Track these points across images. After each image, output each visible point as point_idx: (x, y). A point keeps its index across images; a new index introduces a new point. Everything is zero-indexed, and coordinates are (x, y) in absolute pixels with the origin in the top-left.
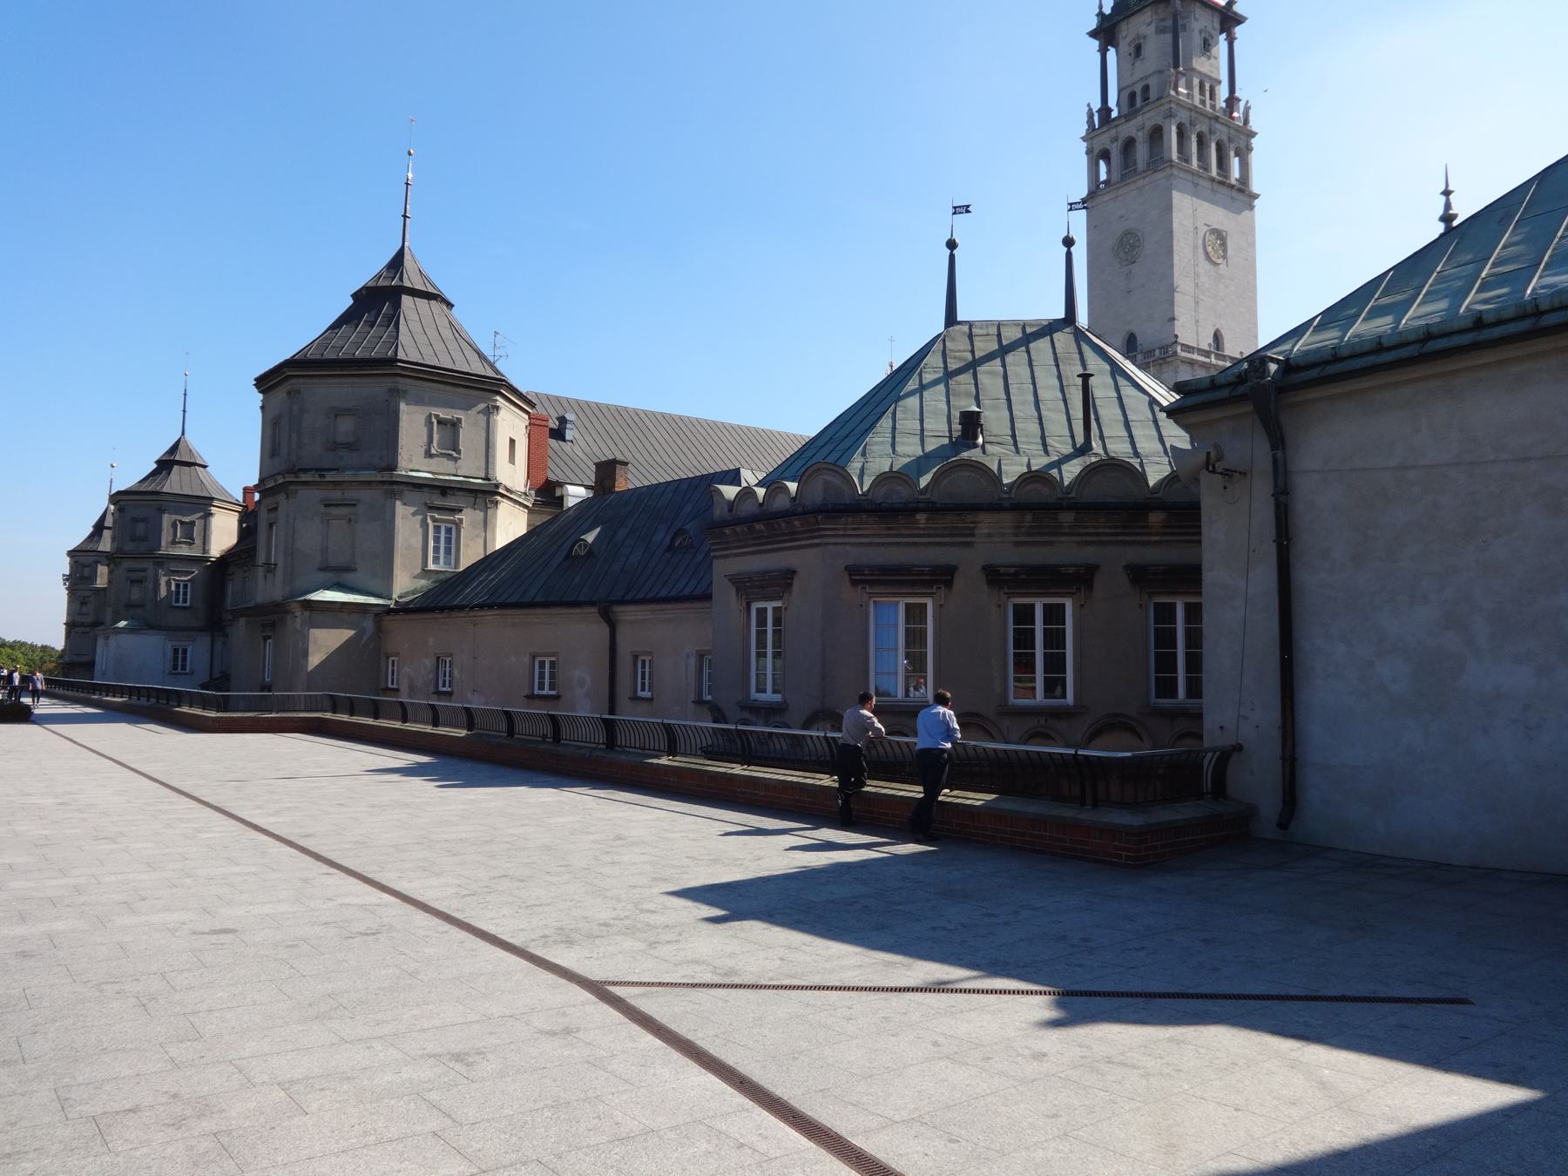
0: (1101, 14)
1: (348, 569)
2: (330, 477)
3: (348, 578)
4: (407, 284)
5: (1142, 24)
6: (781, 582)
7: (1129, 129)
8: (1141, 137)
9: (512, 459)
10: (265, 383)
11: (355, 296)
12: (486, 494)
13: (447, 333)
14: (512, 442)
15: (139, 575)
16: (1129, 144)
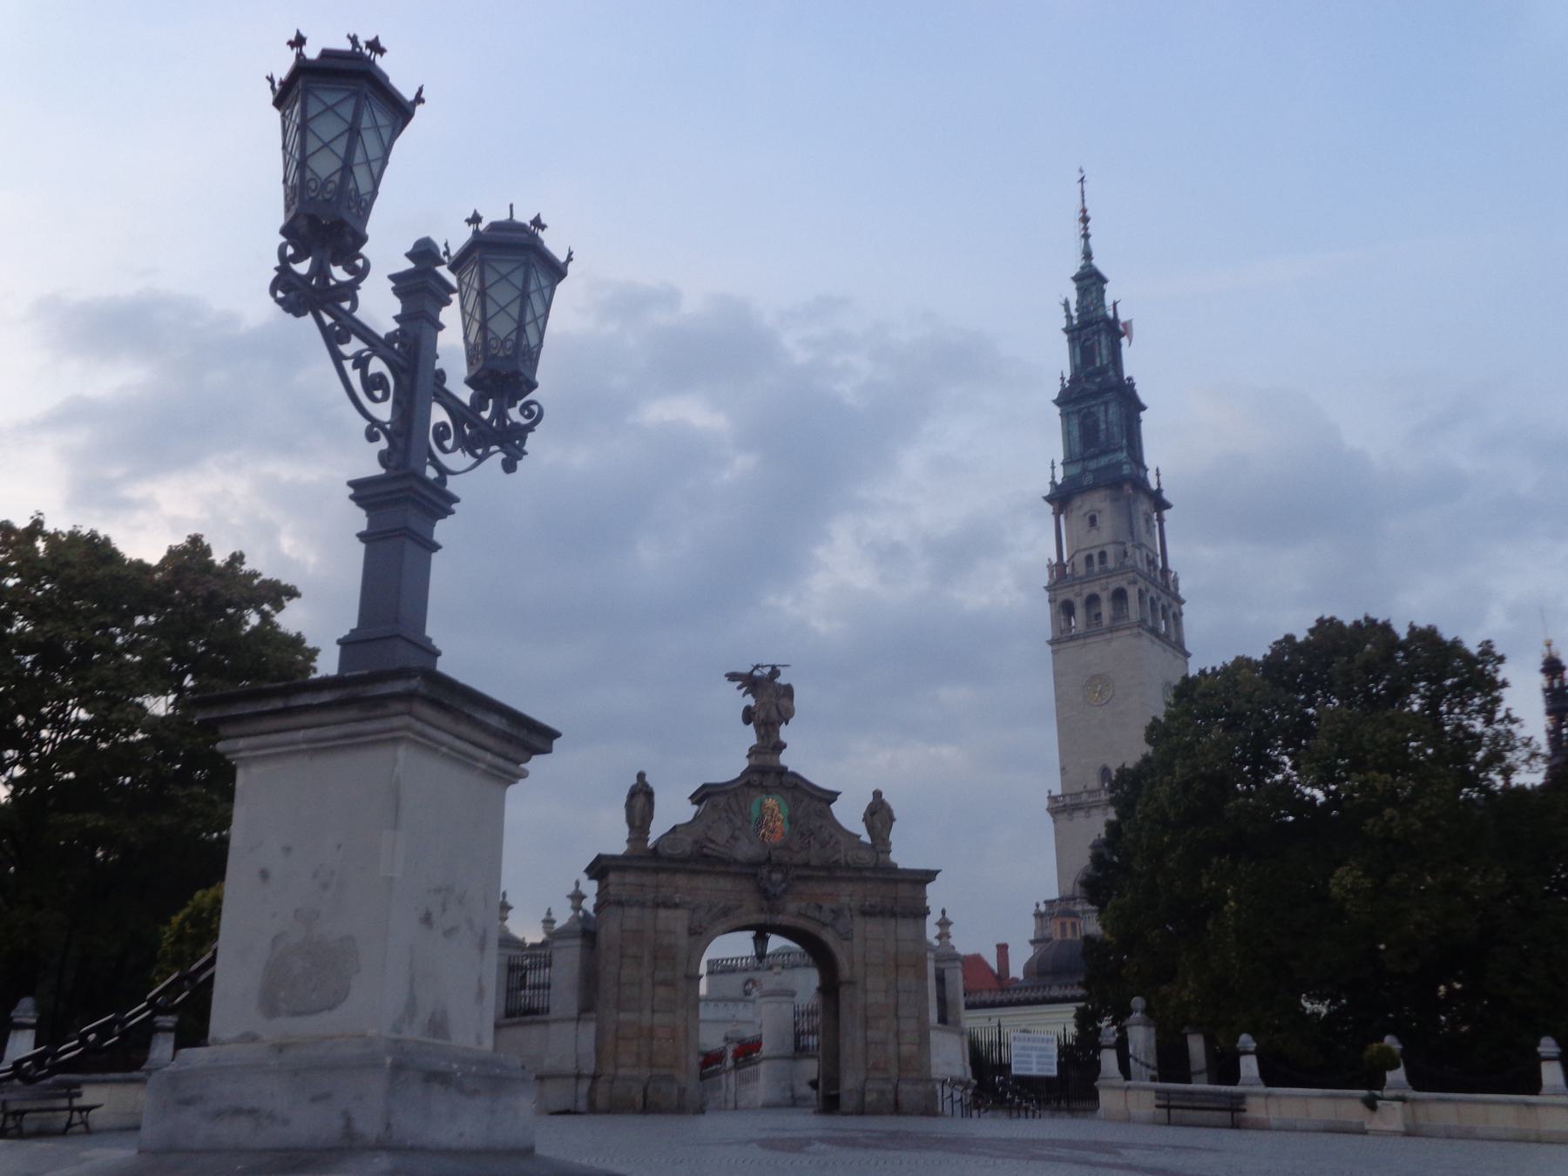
0: (1053, 483)
5: (1098, 502)
8: (1105, 597)
16: (1093, 600)
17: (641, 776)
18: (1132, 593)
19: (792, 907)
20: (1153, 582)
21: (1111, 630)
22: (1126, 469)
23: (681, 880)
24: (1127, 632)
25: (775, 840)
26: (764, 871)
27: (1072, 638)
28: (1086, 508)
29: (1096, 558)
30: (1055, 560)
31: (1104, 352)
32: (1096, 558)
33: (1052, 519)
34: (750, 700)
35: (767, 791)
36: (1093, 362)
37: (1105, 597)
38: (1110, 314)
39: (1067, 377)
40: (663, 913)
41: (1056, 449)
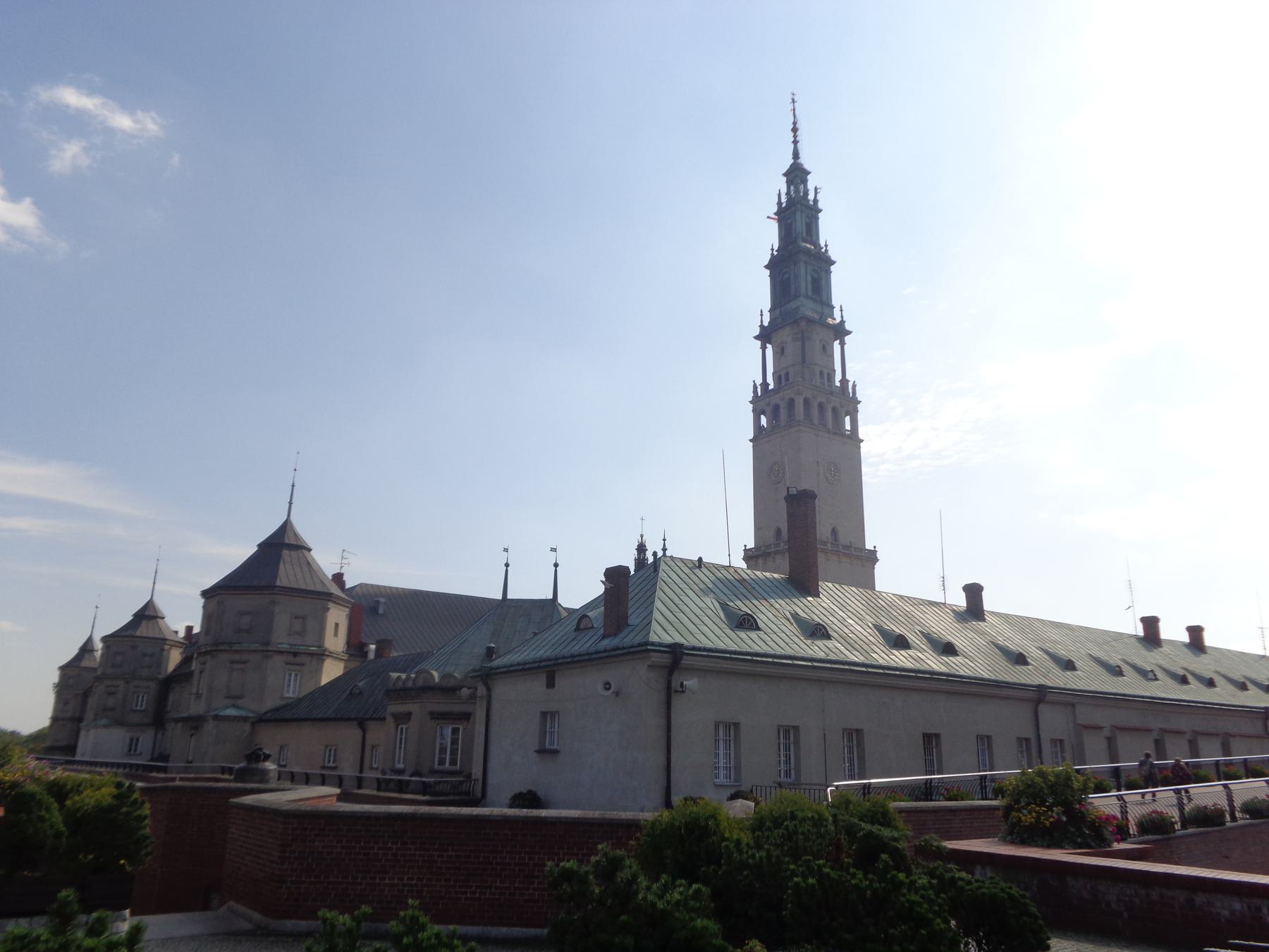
0: (762, 326)
1: (238, 698)
2: (236, 647)
3: (239, 702)
4: (287, 541)
5: (785, 335)
6: (408, 716)
7: (775, 400)
8: (783, 405)
9: (336, 634)
10: (206, 594)
11: (260, 546)
12: (321, 655)
13: (306, 568)
14: (337, 625)
15: (113, 689)
16: (776, 409)
30: (759, 381)
37: (783, 405)
38: (811, 197)
39: (776, 248)
41: (766, 303)
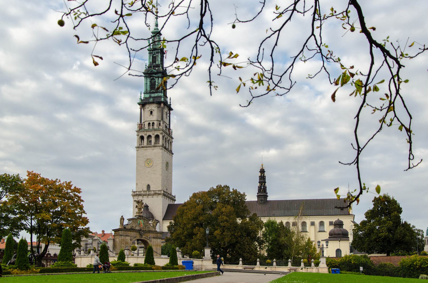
5: (153, 107)
8: (153, 137)
16: (149, 137)
17: (122, 216)
18: (161, 136)
19: (144, 237)
20: (166, 133)
21: (154, 146)
22: (162, 99)
23: (129, 232)
24: (159, 148)
25: (142, 227)
26: (141, 232)
27: (143, 147)
28: (150, 108)
29: (151, 124)
30: (139, 123)
31: (159, 60)
32: (151, 124)
33: (139, 110)
34: (137, 205)
35: (140, 219)
36: (155, 62)
40: (127, 237)
